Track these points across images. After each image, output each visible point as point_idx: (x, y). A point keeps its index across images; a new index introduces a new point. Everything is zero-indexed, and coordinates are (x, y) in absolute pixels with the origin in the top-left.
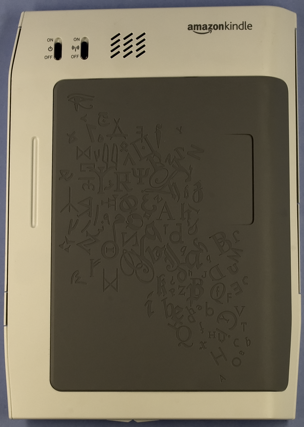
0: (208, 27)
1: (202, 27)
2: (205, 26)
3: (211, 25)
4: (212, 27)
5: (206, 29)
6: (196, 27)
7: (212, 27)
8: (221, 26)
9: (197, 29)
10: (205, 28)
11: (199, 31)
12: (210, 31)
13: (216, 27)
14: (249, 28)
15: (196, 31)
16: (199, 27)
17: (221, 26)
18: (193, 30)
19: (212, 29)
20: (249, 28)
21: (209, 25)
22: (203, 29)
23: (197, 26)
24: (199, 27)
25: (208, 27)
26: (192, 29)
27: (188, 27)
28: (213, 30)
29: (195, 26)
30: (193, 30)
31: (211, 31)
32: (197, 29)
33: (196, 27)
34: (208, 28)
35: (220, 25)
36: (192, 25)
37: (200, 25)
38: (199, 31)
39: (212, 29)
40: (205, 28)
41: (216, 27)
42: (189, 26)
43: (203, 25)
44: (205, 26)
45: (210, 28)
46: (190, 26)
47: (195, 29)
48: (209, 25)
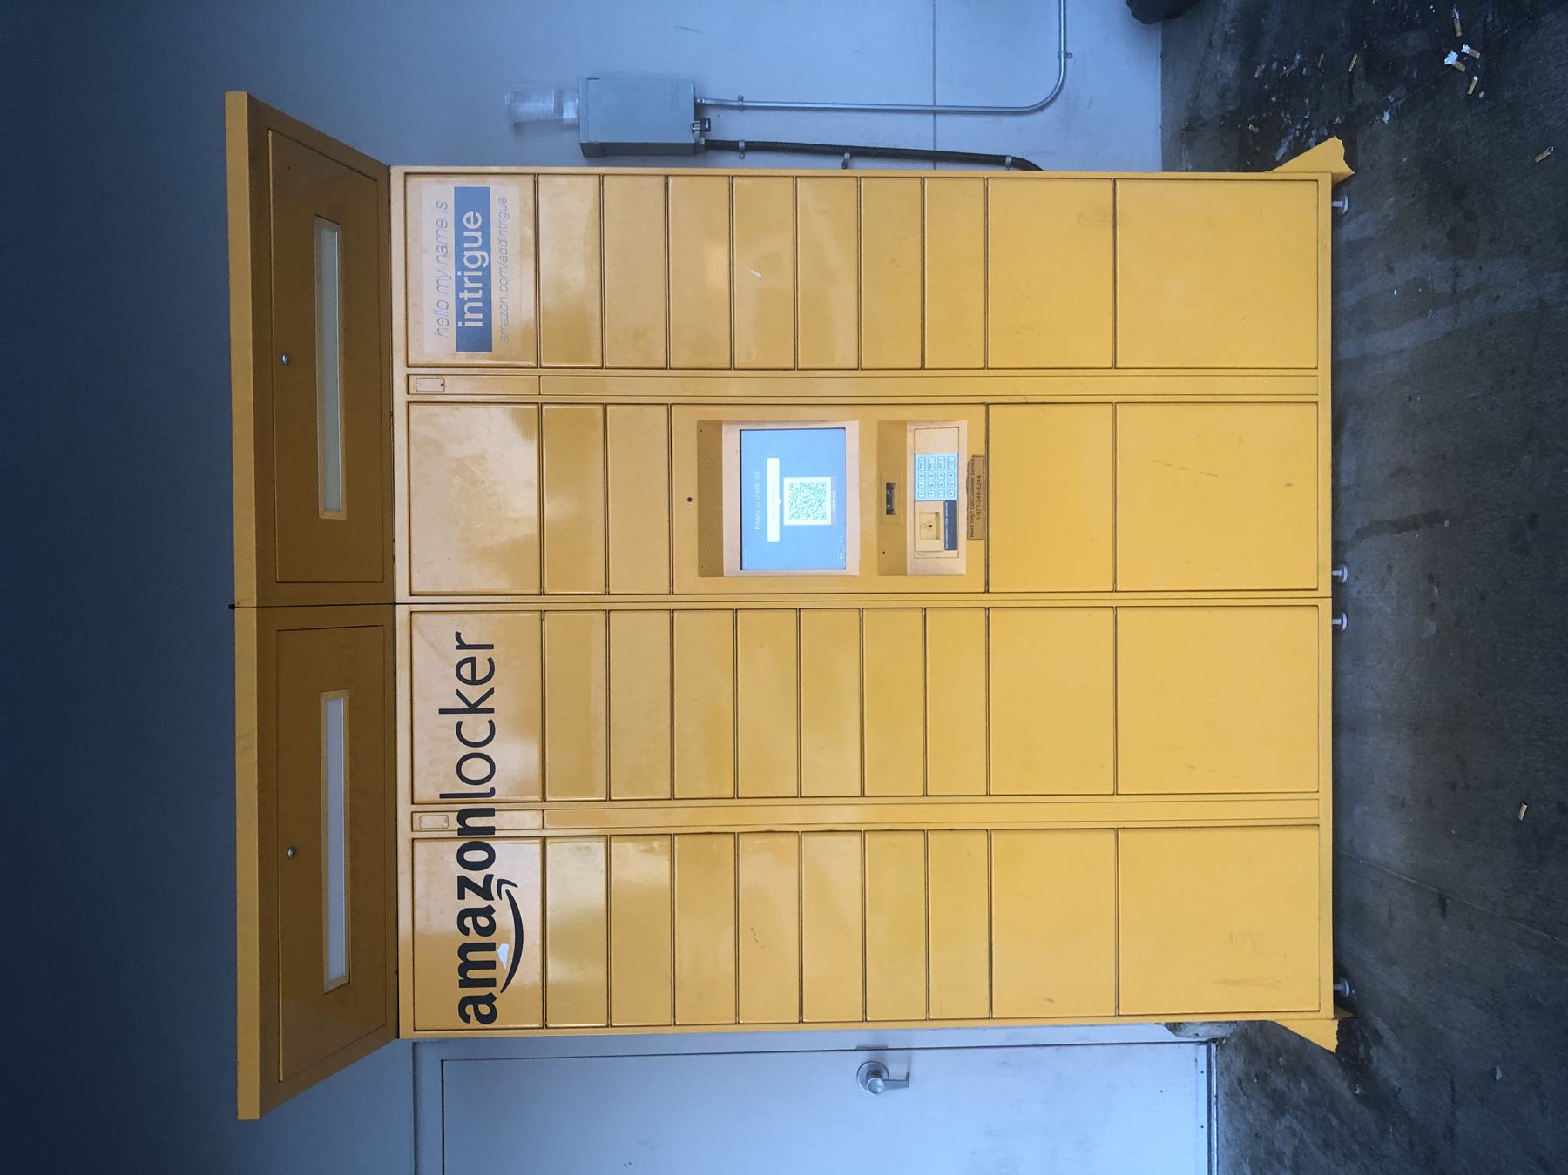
0: (473, 901)
1: (474, 938)
2: (468, 922)
3: (464, 883)
4: (478, 877)
5: (487, 912)
6: (473, 974)
7: (478, 877)
8: (472, 822)
9: (491, 965)
10: (483, 922)
11: (504, 954)
12: (504, 887)
13: (481, 856)
14: (480, 676)
15: (500, 975)
16: (473, 956)
17: (472, 822)
18: (495, 991)
19: (489, 878)
20: (480, 676)
21: (461, 896)
22: (491, 929)
23: (463, 970)
24: (473, 956)
25: (473, 901)
26: (489, 1000)
27: (473, 1018)
28: (497, 870)
29: (466, 983)
30: (495, 991)
31: (501, 882)
32: (491, 965)
33: (473, 974)
34: (482, 903)
35: (464, 830)
36: (464, 1002)
37: (464, 950)
38: (504, 954)
39: (489, 878)
40: (483, 922)
41: (471, 856)
42: (466, 1018)
43: (465, 931)
44: (468, 922)
45: (485, 892)
46: (470, 1010)
47: (491, 983)
48: (461, 896)
